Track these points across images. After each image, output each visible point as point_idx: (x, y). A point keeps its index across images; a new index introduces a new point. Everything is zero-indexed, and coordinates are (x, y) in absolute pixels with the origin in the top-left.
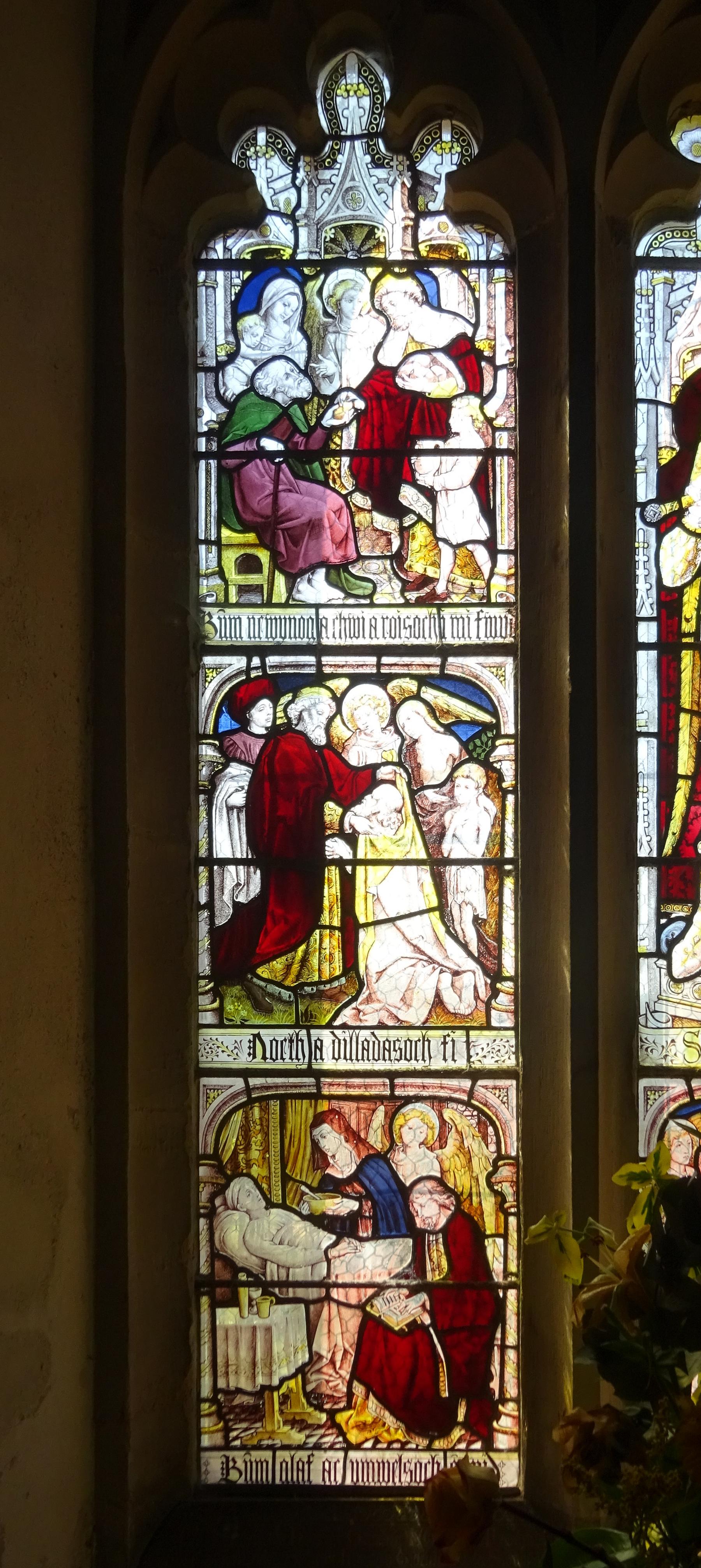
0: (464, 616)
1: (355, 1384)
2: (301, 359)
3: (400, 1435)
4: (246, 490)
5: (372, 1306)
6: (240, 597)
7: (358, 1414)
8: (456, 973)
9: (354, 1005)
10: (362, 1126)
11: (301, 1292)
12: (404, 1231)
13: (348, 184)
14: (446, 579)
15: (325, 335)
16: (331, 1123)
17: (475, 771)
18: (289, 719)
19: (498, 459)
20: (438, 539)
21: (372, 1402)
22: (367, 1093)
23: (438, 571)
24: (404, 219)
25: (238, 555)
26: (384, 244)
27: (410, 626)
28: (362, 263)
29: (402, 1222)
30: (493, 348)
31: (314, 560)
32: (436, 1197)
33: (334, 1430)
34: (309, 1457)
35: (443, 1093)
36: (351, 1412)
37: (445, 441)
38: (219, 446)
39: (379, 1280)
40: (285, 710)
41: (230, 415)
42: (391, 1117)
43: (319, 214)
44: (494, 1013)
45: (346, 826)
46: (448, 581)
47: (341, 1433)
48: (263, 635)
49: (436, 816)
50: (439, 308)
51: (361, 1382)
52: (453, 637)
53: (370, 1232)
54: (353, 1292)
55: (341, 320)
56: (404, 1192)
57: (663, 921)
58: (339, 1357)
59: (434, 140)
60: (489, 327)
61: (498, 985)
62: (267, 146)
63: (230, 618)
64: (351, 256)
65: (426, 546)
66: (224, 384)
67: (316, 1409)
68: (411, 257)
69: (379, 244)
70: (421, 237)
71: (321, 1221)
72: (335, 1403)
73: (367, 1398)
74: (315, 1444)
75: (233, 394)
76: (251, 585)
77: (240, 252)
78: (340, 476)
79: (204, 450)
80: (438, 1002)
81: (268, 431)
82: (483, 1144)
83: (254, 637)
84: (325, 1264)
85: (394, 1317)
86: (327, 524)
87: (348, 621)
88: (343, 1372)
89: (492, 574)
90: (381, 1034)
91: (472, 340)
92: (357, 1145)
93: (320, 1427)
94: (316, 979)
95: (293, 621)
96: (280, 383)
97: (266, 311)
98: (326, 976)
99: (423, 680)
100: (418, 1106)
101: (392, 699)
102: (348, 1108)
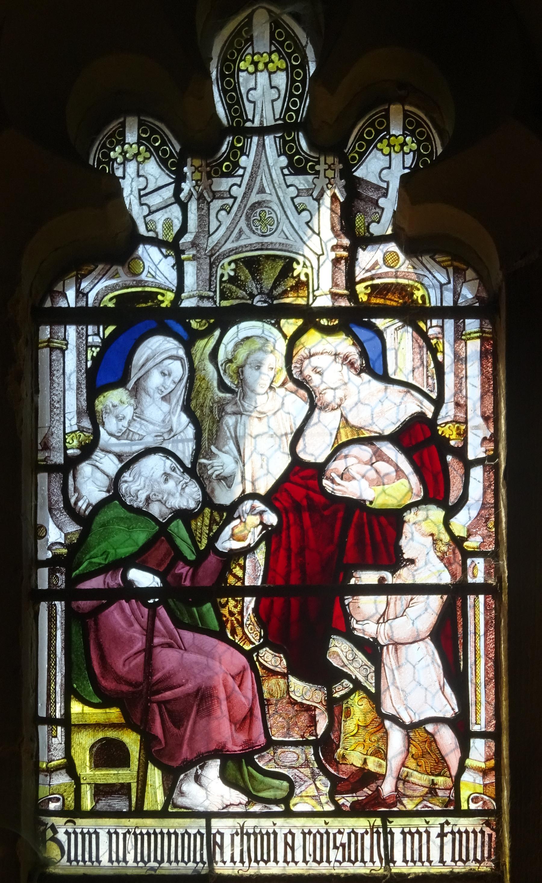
0: (422, 830)
4: (107, 645)
6: (97, 802)
13: (254, 198)
14: (395, 775)
15: (221, 418)
19: (471, 599)
20: (384, 717)
23: (384, 763)
24: (333, 248)
25: (93, 741)
26: (306, 284)
27: (343, 845)
30: (464, 435)
37: (393, 573)
38: (68, 580)
41: (84, 535)
46: (398, 779)
48: (130, 857)
52: (405, 861)
55: (244, 396)
59: (378, 133)
60: (457, 404)
62: (139, 144)
63: (82, 833)
64: (258, 302)
65: (366, 727)
66: (76, 490)
68: (344, 303)
70: (360, 274)
75: (89, 505)
76: (113, 785)
77: (99, 297)
78: (241, 624)
79: (46, 586)
83: (118, 861)
86: (222, 696)
87: (252, 837)
89: (462, 768)
91: (432, 423)
95: (173, 837)
96: (156, 487)
97: (136, 383)
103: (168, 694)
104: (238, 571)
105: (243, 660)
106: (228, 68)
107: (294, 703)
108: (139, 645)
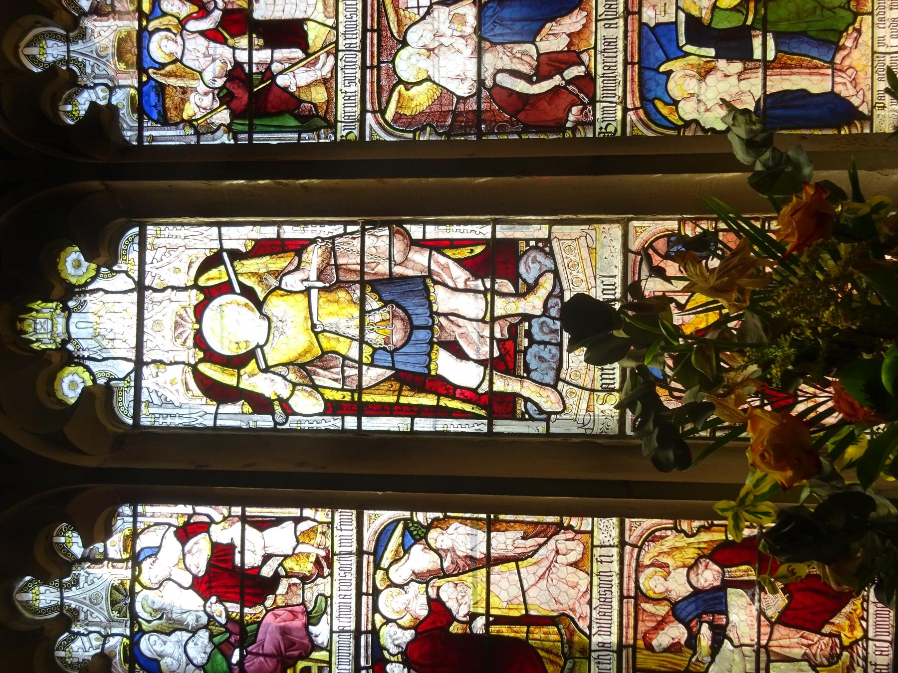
1: (823, 631)
2: (186, 635)
3: (858, 602)
5: (772, 617)
7: (844, 630)
8: (557, 552)
9: (576, 620)
10: (654, 618)
11: (763, 665)
12: (722, 594)
13: (88, 602)
15: (173, 619)
16: (651, 639)
17: (433, 535)
18: (398, 653)
19: (247, 514)
20: (293, 553)
21: (835, 620)
22: (633, 614)
24: (108, 568)
26: (122, 580)
28: (132, 594)
29: (716, 594)
30: (183, 515)
31: (304, 633)
32: (700, 571)
33: (854, 647)
34: (872, 665)
35: (634, 564)
36: (842, 635)
37: (236, 547)
39: (755, 613)
40: (394, 655)
42: (649, 599)
43: (103, 619)
44: (583, 529)
45: (465, 619)
47: (856, 642)
48: (348, 667)
49: (459, 561)
50: (159, 548)
51: (823, 627)
53: (723, 616)
54: (763, 630)
55: (165, 609)
56: (697, 592)
57: (527, 416)
58: (805, 641)
59: (64, 548)
60: (171, 517)
61: (565, 525)
62: (65, 651)
64: (128, 601)
67: (840, 659)
68: (130, 563)
69: (122, 583)
70: (118, 557)
71: (716, 648)
72: (837, 645)
73: (833, 624)
74: (863, 660)
78: (255, 614)
80: (575, 565)
81: (228, 658)
82: (666, 539)
84: (744, 648)
85: (779, 602)
86: (283, 624)
88: (816, 639)
89: (314, 520)
90: (595, 603)
92: (666, 623)
93: (852, 657)
94: (559, 644)
96: (200, 649)
97: (158, 656)
98: (557, 637)
99: (377, 566)
100: (641, 581)
101: (388, 587)
102: (642, 628)
103: (282, 648)
104: (234, 615)
105: (270, 613)
106: (38, 611)
107: (287, 593)
108: (262, 659)
